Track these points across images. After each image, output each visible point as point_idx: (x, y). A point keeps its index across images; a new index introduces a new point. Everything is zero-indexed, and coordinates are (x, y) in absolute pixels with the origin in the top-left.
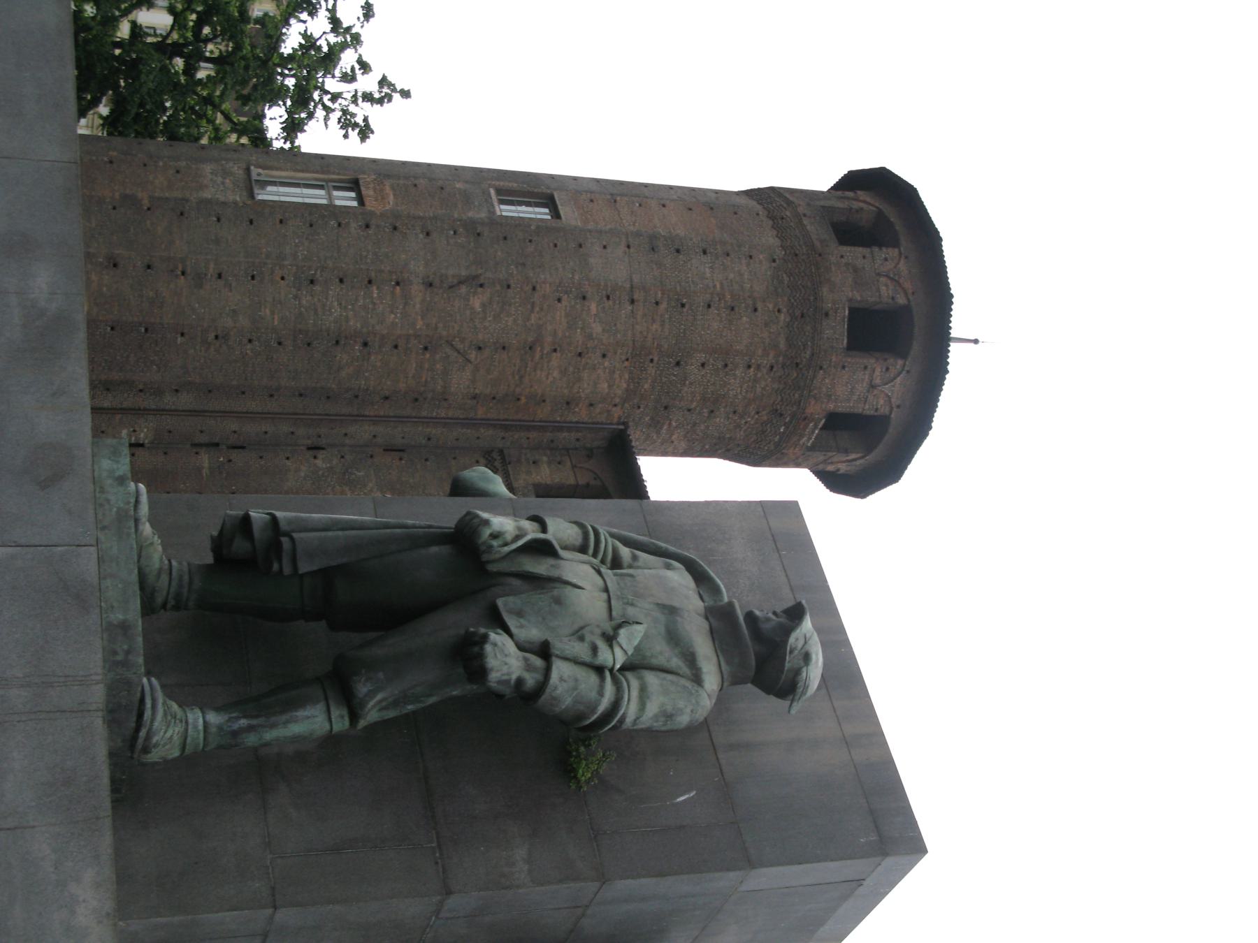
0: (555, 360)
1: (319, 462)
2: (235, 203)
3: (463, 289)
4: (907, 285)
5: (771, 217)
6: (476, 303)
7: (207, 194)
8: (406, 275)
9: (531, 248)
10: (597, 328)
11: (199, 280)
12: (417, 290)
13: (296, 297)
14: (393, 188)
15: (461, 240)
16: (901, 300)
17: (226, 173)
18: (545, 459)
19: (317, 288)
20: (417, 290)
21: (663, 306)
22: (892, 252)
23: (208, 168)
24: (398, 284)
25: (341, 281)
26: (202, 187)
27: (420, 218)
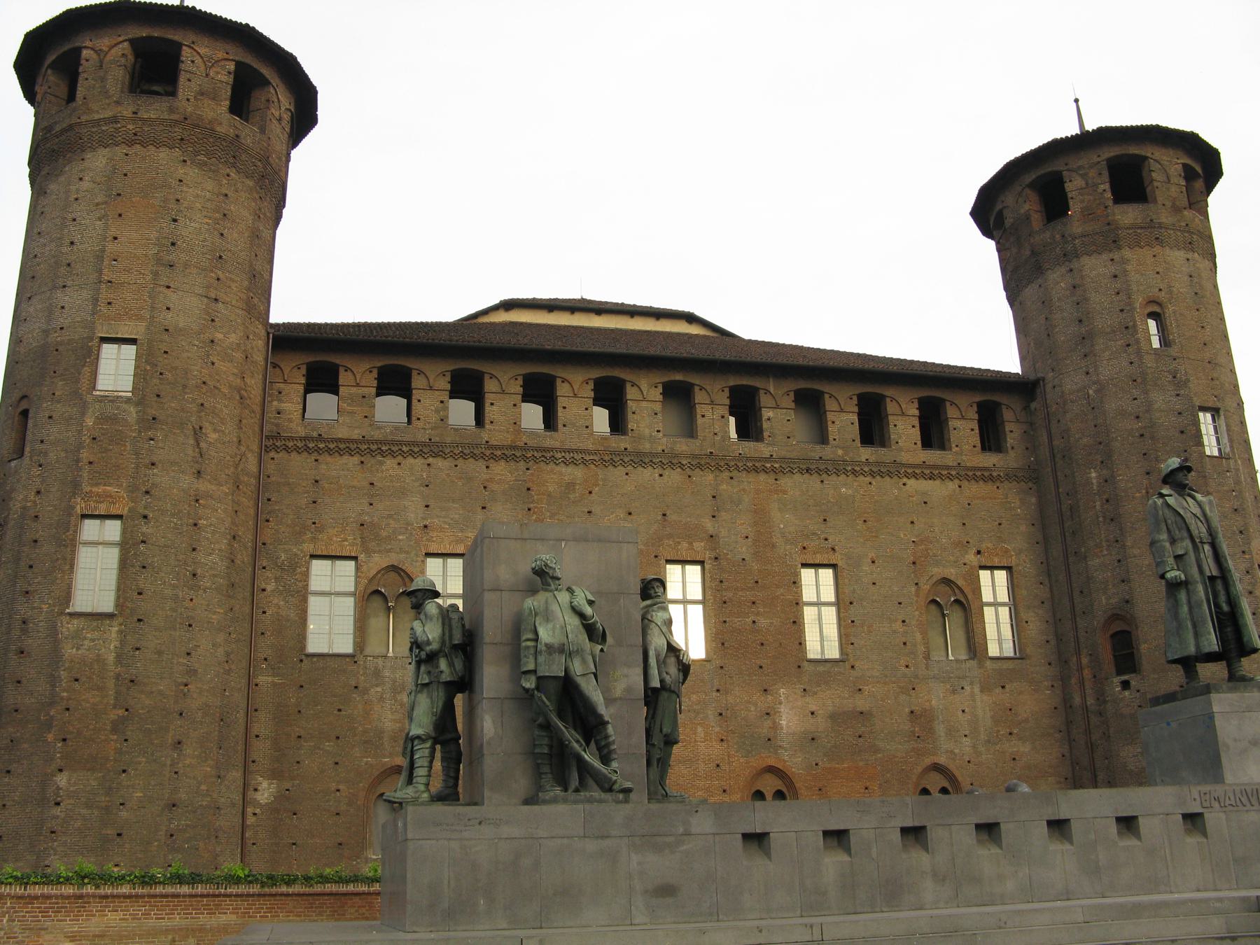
0: (248, 380)
1: (269, 588)
2: (120, 632)
3: (203, 445)
4: (221, 55)
5: (130, 143)
6: (213, 436)
7: (111, 658)
8: (192, 493)
9: (168, 375)
10: (233, 338)
11: (192, 672)
12: (203, 486)
13: (205, 591)
14: (97, 485)
15: (160, 435)
16: (231, 66)
17: (77, 635)
18: (275, 403)
19: (199, 571)
20: (203, 486)
21: (221, 276)
22: (186, 52)
23: (69, 651)
24: (197, 501)
25: (194, 550)
26: (99, 660)
27: (137, 467)
